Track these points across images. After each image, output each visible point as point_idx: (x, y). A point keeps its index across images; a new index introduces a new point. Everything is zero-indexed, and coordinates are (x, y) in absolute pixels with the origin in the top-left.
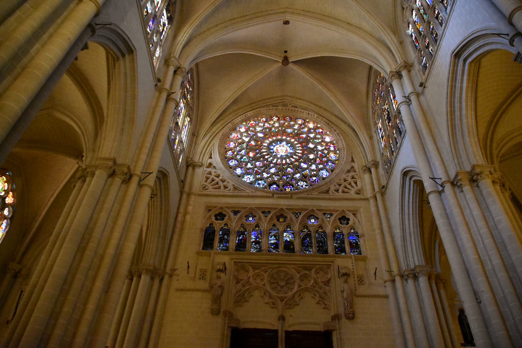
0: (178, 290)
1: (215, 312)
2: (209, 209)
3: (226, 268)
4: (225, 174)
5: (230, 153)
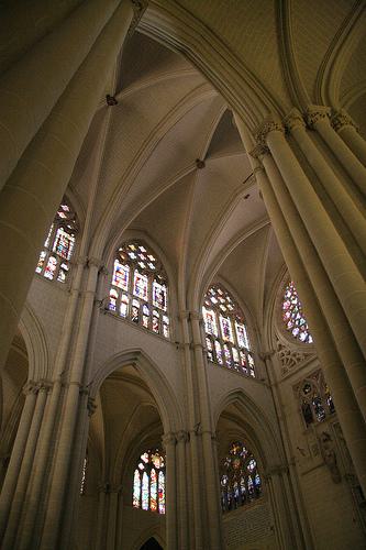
0: (304, 474)
1: (337, 480)
2: (295, 388)
3: (328, 436)
4: (293, 348)
5: (290, 324)
